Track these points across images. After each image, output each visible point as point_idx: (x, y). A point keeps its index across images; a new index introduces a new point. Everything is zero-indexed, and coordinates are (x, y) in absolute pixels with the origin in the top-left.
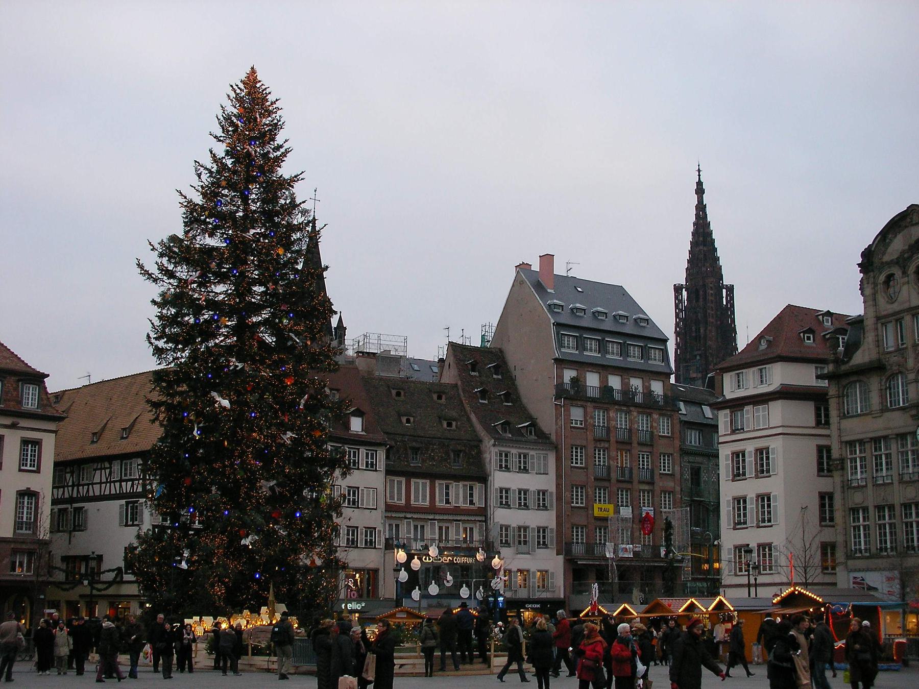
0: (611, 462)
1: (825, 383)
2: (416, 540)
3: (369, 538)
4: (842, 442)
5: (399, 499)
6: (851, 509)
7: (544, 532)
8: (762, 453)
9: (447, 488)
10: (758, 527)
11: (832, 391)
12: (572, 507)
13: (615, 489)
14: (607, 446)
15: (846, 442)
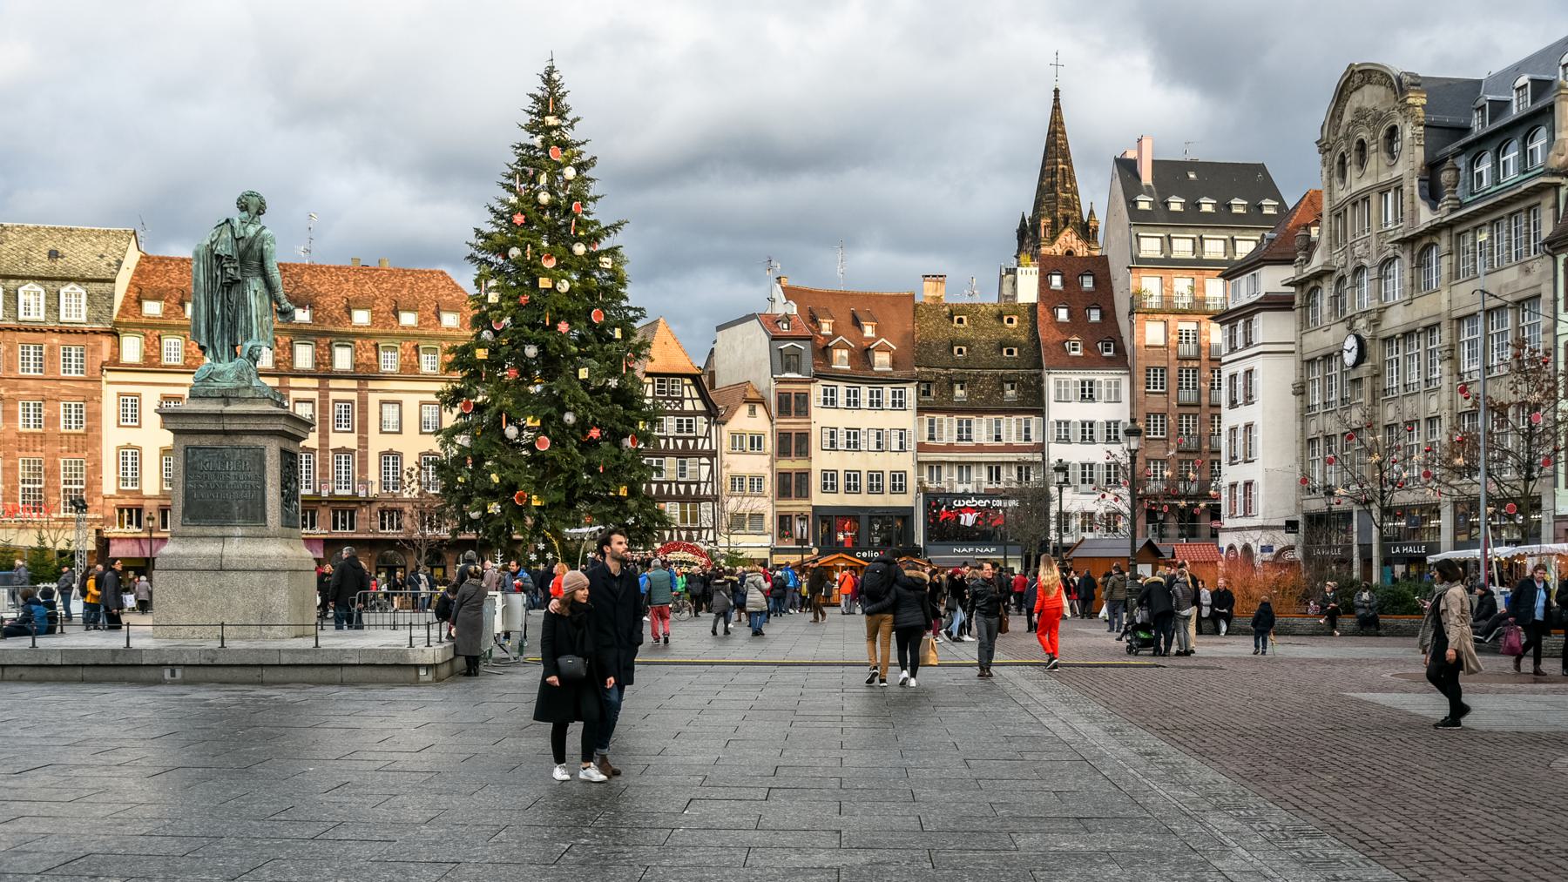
0: (1203, 385)
1: (1292, 289)
2: (960, 481)
3: (898, 483)
4: (1303, 361)
5: (941, 439)
6: (1310, 440)
7: (1116, 468)
8: (1249, 372)
9: (998, 423)
10: (1246, 462)
11: (1297, 301)
12: (1146, 439)
13: (1208, 416)
14: (1196, 364)
15: (1308, 361)
